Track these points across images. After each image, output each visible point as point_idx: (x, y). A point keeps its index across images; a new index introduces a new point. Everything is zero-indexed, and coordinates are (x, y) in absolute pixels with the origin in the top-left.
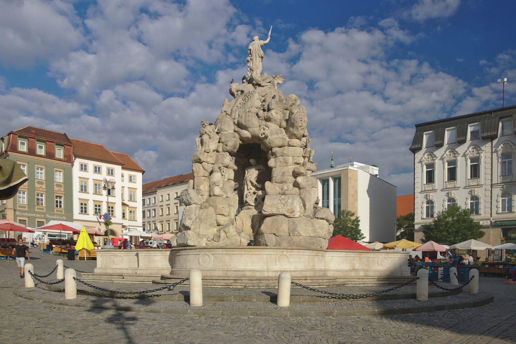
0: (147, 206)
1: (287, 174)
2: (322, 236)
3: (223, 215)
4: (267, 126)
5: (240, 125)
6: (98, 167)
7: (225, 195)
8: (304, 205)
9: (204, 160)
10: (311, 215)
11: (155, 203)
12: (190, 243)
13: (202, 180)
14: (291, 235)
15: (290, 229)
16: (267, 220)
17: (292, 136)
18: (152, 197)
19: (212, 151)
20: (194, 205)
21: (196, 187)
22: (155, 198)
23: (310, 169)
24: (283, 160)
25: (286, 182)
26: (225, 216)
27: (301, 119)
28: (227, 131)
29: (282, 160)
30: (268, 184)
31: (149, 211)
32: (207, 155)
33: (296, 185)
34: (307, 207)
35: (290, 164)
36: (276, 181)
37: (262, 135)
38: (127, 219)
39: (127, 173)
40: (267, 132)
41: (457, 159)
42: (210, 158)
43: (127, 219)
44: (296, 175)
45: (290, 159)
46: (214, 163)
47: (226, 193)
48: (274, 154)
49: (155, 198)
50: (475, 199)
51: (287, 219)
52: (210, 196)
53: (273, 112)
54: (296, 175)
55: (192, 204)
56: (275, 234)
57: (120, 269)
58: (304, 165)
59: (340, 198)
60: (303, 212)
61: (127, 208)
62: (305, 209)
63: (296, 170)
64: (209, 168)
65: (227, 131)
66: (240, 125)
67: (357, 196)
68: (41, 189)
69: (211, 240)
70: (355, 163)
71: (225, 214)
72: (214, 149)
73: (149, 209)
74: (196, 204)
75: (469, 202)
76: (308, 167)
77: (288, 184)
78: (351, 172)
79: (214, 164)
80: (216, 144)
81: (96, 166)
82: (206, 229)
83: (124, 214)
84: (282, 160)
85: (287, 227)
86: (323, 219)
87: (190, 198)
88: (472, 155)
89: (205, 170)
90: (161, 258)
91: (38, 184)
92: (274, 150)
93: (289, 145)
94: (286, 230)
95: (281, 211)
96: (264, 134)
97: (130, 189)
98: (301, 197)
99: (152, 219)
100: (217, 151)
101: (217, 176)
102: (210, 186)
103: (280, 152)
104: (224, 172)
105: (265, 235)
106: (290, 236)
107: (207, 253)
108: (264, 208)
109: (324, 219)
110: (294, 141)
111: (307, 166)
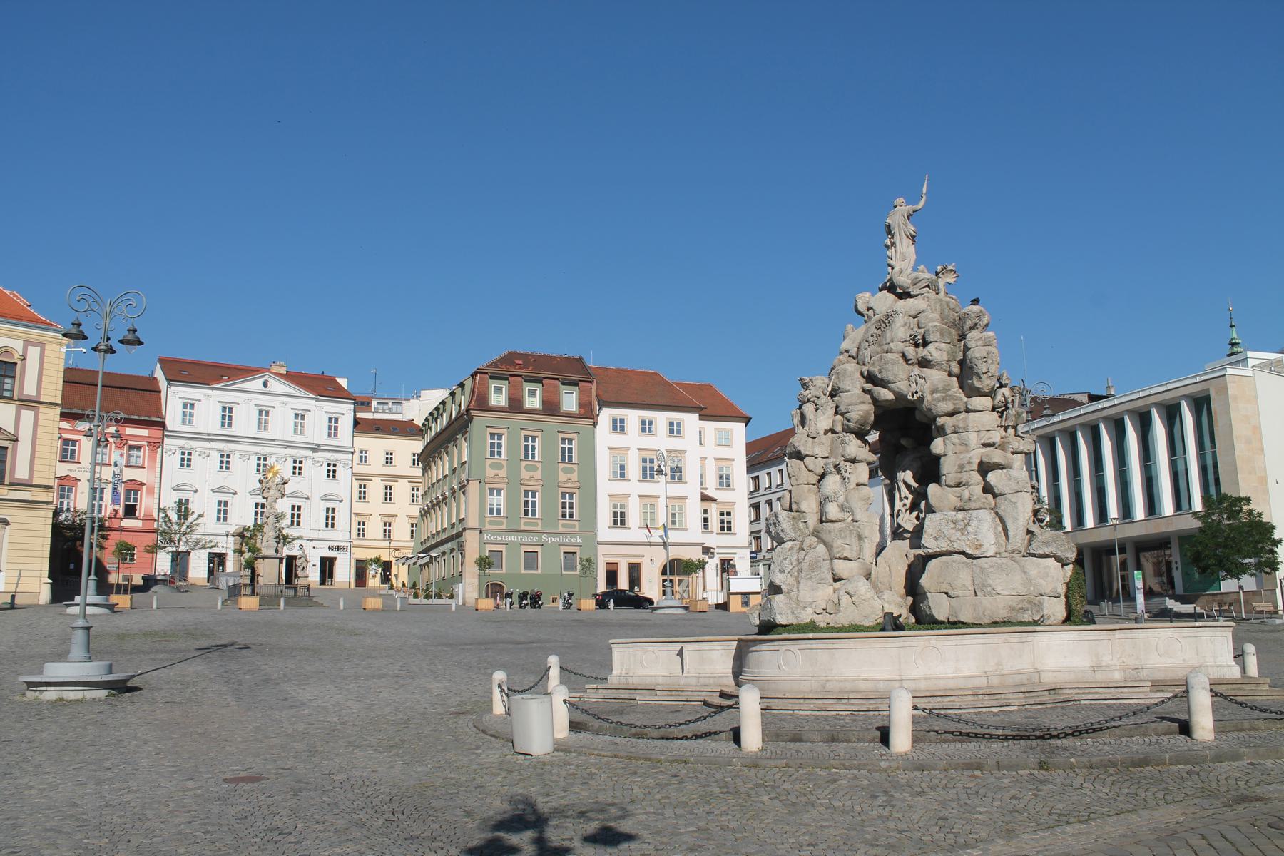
0: (765, 493)
1: (967, 467)
2: (1047, 591)
3: (845, 558)
4: (921, 377)
5: (870, 378)
7: (851, 518)
8: (1005, 531)
9: (808, 453)
10: (1023, 549)
12: (780, 620)
13: (806, 491)
14: (978, 593)
15: (976, 583)
16: (932, 564)
17: (973, 392)
18: (774, 470)
19: (822, 432)
20: (789, 544)
21: (794, 507)
23: (1019, 450)
24: (959, 439)
25: (967, 484)
26: (851, 560)
27: (985, 360)
29: (956, 441)
30: (932, 488)
31: (769, 503)
32: (813, 442)
33: (987, 489)
34: (1011, 534)
35: (972, 447)
36: (947, 483)
37: (913, 396)
38: (712, 532)
39: (711, 426)
40: (925, 388)
43: (712, 532)
44: (984, 469)
45: (973, 439)
46: (827, 455)
47: (853, 514)
48: (942, 432)
51: (969, 560)
52: (821, 522)
53: (931, 347)
54: (984, 469)
55: (785, 542)
56: (946, 593)
57: (651, 676)
58: (1002, 446)
59: (1215, 448)
60: (1004, 544)
62: (1007, 538)
63: (985, 460)
64: (818, 465)
66: (870, 378)
67: (1261, 440)
68: (532, 482)
69: (822, 611)
70: (1250, 354)
71: (849, 556)
72: (828, 428)
73: (768, 498)
74: (794, 541)
77: (971, 487)
78: (1234, 382)
79: (827, 457)
82: (813, 590)
83: (706, 520)
84: (956, 441)
85: (970, 578)
86: (1046, 556)
87: (782, 531)
89: (810, 471)
90: (722, 655)
91: (527, 471)
92: (940, 421)
93: (968, 411)
94: (969, 584)
96: (917, 393)
97: (720, 462)
98: (997, 514)
100: (834, 432)
101: (832, 482)
102: (821, 502)
103: (951, 425)
104: (848, 472)
105: (929, 595)
106: (976, 596)
107: (792, 648)
108: (923, 542)
109: (1051, 557)
110: (978, 402)
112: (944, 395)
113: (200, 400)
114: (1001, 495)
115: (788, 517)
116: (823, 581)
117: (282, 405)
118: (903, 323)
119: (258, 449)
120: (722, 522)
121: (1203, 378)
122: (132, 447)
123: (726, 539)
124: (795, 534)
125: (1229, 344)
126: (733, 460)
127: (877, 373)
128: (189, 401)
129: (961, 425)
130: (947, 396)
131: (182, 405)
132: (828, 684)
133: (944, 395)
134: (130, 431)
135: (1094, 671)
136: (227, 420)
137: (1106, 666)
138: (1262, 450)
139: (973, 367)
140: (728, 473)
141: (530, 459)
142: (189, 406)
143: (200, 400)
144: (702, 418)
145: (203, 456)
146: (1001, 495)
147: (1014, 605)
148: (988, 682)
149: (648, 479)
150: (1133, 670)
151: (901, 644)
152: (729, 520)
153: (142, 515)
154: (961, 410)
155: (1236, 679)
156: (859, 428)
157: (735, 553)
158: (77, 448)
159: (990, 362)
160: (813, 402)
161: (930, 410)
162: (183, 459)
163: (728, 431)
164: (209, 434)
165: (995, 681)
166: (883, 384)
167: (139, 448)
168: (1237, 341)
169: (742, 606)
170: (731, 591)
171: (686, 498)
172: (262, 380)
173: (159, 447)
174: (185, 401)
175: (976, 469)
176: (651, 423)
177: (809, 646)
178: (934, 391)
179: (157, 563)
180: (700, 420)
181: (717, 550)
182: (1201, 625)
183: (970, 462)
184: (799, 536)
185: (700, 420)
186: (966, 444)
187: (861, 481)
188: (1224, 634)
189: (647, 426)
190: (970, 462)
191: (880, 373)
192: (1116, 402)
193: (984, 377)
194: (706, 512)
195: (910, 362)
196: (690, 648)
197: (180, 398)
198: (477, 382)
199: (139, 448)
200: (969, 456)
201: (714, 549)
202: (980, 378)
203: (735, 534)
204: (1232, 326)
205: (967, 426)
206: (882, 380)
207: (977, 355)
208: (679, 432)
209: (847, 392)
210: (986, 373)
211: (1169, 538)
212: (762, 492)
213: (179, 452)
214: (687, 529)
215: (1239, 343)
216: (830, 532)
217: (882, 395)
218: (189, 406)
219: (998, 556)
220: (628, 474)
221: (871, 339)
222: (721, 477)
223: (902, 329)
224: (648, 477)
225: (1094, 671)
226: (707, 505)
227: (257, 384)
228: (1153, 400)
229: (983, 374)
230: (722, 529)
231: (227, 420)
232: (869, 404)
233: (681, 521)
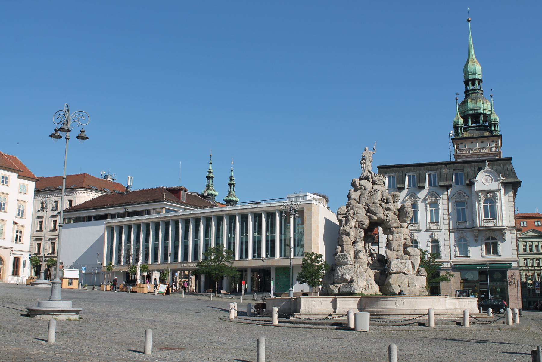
1: (401, 246)
5: (368, 211)
14: (410, 286)
15: (409, 283)
25: (400, 251)
28: (361, 214)
41: (418, 203)
42: (353, 232)
50: (435, 242)
56: (399, 286)
65: (361, 214)
70: (308, 194)
75: (430, 244)
84: (397, 236)
87: (348, 261)
88: (431, 201)
92: (393, 229)
95: (403, 271)
97: (20, 202)
103: (396, 231)
114: (412, 255)
120: (17, 236)
121: (302, 203)
125: (208, 172)
127: (374, 210)
129: (400, 232)
130: (396, 221)
132: (416, 311)
138: (319, 235)
139: (407, 214)
140: (23, 209)
144: (20, 177)
146: (412, 255)
147: (421, 290)
152: (20, 236)
160: (351, 216)
161: (390, 225)
163: (26, 186)
166: (375, 214)
168: (212, 171)
169: (69, 285)
170: (64, 277)
177: (409, 299)
179: (257, 261)
180: (18, 178)
183: (402, 244)
185: (18, 178)
186: (400, 238)
191: (375, 210)
192: (262, 206)
193: (409, 217)
195: (383, 208)
196: (340, 300)
202: (408, 218)
203: (23, 244)
204: (210, 163)
206: (375, 213)
207: (409, 211)
209: (360, 214)
211: (271, 268)
214: (4, 239)
215: (212, 172)
216: (361, 262)
217: (374, 218)
221: (366, 197)
222: (19, 211)
228: (277, 208)
230: (16, 240)
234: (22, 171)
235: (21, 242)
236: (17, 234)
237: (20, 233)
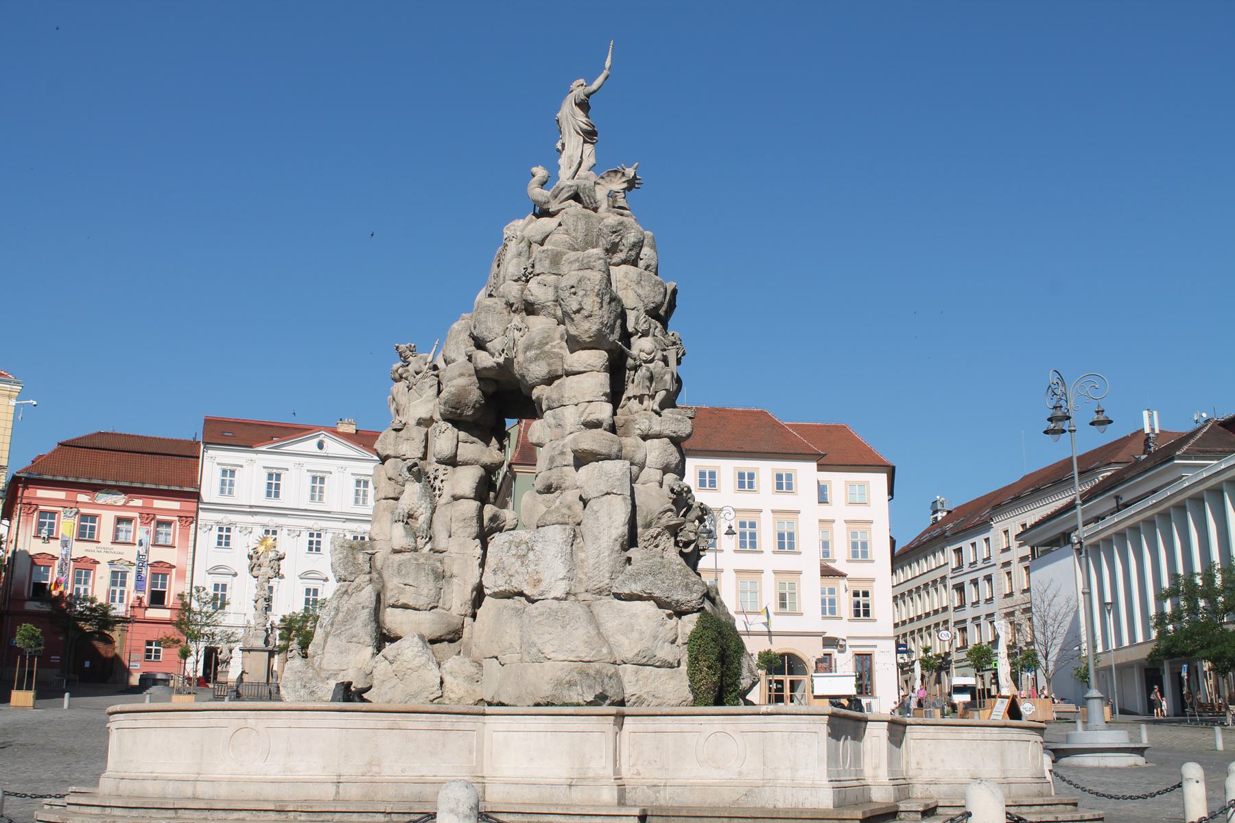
0: (970, 570)
1: (558, 461)
3: (405, 607)
6: (710, 473)
7: (429, 546)
11: (989, 558)
18: (979, 540)
19: (412, 422)
22: (987, 540)
24: (555, 419)
31: (975, 582)
35: (569, 429)
39: (838, 481)
49: (987, 540)
61: (842, 582)
71: (411, 603)
73: (973, 576)
76: (643, 427)
80: (429, 401)
81: (742, 471)
99: (983, 610)
111: (637, 426)
112: (538, 352)
113: (242, 466)
115: (342, 546)
116: (354, 639)
117: (340, 469)
118: (516, 253)
119: (310, 523)
122: (43, 514)
123: (862, 628)
124: (345, 569)
126: (871, 522)
128: (229, 468)
131: (220, 472)
133: (538, 352)
134: (158, 503)
135: (570, 786)
136: (273, 489)
137: (595, 779)
141: (317, 500)
142: (228, 473)
143: (242, 466)
144: (821, 467)
145: (245, 532)
148: (338, 793)
149: (748, 548)
150: (648, 787)
151: (204, 723)
152: (867, 602)
153: (171, 604)
154: (560, 373)
155: (825, 811)
156: (451, 412)
157: (875, 646)
158: (56, 521)
159: (581, 293)
162: (220, 537)
163: (862, 485)
164: (251, 507)
165: (352, 792)
167: (169, 524)
171: (800, 573)
172: (316, 441)
173: (192, 522)
174: (223, 467)
175: (572, 462)
176: (751, 476)
178: (528, 348)
180: (818, 470)
181: (849, 643)
182: (769, 711)
183: (562, 453)
184: (351, 573)
185: (818, 470)
187: (459, 492)
188: (813, 727)
189: (746, 480)
190: (562, 453)
194: (832, 591)
197: (218, 464)
198: (522, 429)
199: (169, 524)
200: (562, 443)
201: (844, 640)
205: (563, 397)
208: (790, 487)
210: (578, 311)
212: (966, 568)
213: (216, 529)
214: (801, 614)
218: (228, 473)
219: (572, 598)
220: (871, 553)
222: (854, 545)
223: (515, 261)
224: (860, 557)
225: (570, 786)
226: (831, 582)
227: (310, 445)
229: (575, 313)
230: (857, 614)
231: (273, 489)
232: (469, 375)
233: (793, 604)
234: (826, 455)
235: (869, 616)
236: (857, 598)
237: (863, 596)
